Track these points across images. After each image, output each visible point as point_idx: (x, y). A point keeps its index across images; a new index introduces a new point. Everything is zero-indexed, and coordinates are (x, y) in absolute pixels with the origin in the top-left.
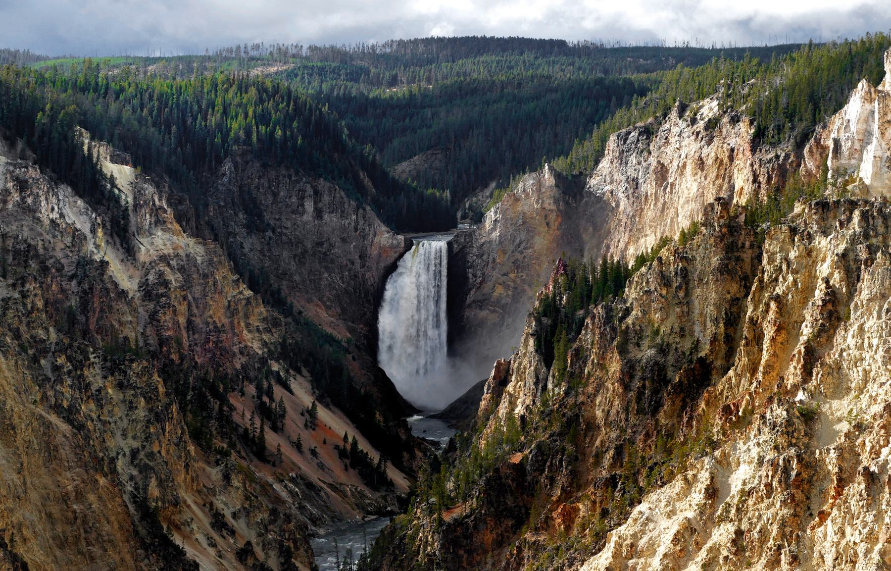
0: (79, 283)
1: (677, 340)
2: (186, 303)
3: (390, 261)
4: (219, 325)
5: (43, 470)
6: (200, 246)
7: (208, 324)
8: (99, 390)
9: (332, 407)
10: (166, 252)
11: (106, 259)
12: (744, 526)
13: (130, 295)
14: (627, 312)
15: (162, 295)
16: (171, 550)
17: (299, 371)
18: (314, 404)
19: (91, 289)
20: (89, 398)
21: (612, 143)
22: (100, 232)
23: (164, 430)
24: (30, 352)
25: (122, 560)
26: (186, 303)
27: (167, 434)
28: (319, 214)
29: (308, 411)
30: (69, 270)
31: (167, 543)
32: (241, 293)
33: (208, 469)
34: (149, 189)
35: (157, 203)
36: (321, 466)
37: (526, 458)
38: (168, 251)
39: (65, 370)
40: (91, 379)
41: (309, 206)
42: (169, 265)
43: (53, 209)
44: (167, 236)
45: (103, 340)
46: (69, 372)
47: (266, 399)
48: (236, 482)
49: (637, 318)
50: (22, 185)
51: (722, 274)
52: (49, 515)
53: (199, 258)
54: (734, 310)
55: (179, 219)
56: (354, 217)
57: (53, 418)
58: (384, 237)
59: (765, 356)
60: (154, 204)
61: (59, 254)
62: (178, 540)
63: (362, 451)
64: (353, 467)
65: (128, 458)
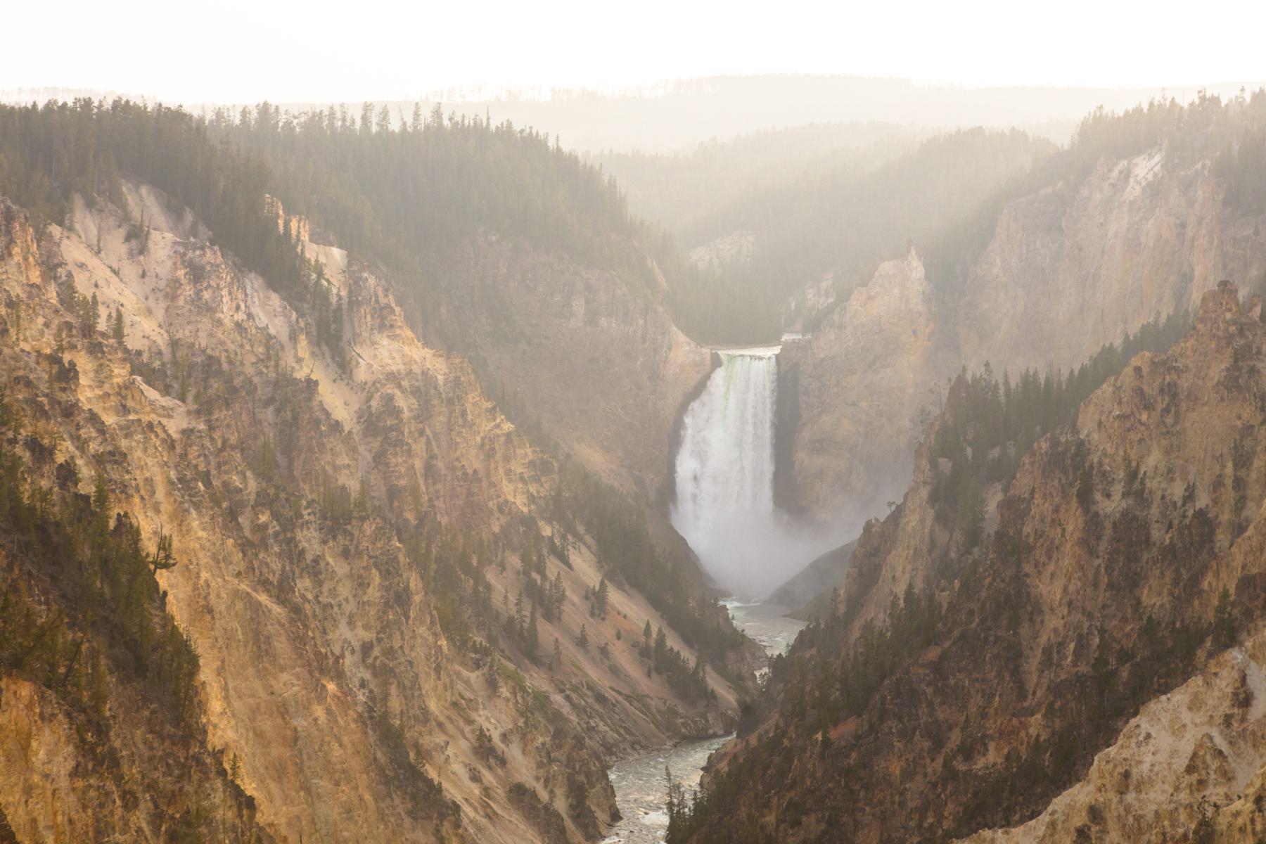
0: (278, 411)
1: (1164, 485)
2: (423, 440)
4: (470, 471)
5: (251, 671)
6: (441, 360)
7: (453, 469)
8: (316, 561)
9: (627, 587)
10: (394, 368)
11: (314, 377)
13: (347, 429)
15: (391, 429)
16: (421, 784)
17: (580, 539)
18: (602, 583)
19: (295, 418)
20: (303, 570)
22: (303, 341)
23: (407, 618)
24: (224, 505)
25: (361, 799)
26: (423, 440)
27: (410, 622)
29: (594, 593)
30: (261, 393)
31: (416, 774)
32: (498, 426)
33: (466, 673)
35: (383, 301)
36: (615, 671)
38: (397, 366)
39: (271, 531)
40: (306, 545)
41: (579, 306)
42: (399, 386)
43: (238, 308)
44: (395, 345)
45: (312, 491)
46: (276, 534)
47: (535, 576)
48: (504, 691)
50: (197, 274)
51: (1230, 391)
52: (259, 735)
53: (440, 378)
57: (263, 598)
60: (377, 301)
61: (249, 370)
63: (672, 649)
64: (659, 672)
65: (358, 655)
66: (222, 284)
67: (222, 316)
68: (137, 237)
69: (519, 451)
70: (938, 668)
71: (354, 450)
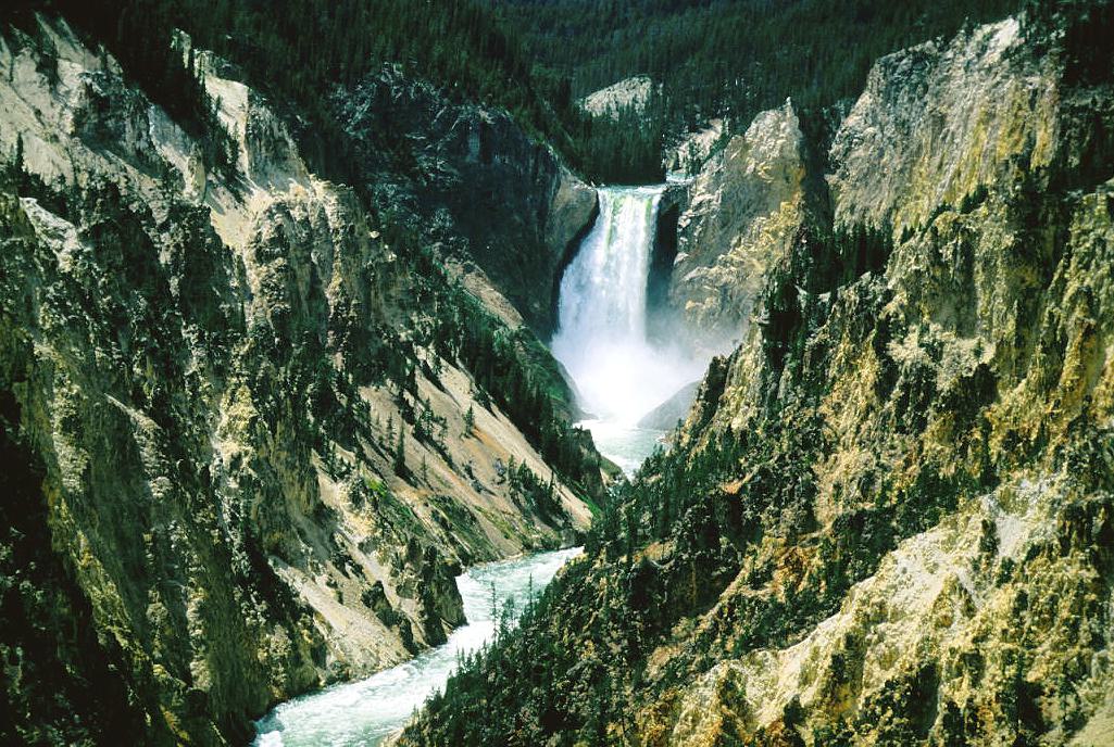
3: (580, 219)
12: (1028, 588)
13: (237, 253)
14: (889, 296)
17: (452, 362)
21: (876, 73)
23: (274, 432)
27: (277, 436)
28: (486, 155)
32: (381, 255)
34: (265, 113)
35: (277, 134)
37: (743, 489)
41: (474, 144)
43: (140, 137)
47: (407, 395)
49: (902, 306)
53: (329, 210)
54: (1030, 303)
55: (302, 154)
56: (532, 161)
58: (571, 188)
59: (1070, 364)
60: (272, 134)
62: (285, 573)
66: (125, 114)
67: (125, 144)
68: (49, 68)
69: (400, 278)
70: (734, 500)
71: (242, 272)
